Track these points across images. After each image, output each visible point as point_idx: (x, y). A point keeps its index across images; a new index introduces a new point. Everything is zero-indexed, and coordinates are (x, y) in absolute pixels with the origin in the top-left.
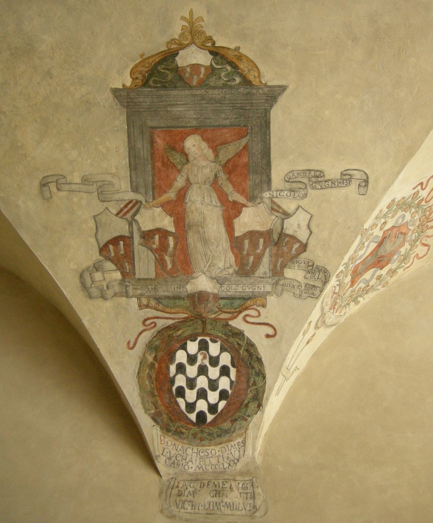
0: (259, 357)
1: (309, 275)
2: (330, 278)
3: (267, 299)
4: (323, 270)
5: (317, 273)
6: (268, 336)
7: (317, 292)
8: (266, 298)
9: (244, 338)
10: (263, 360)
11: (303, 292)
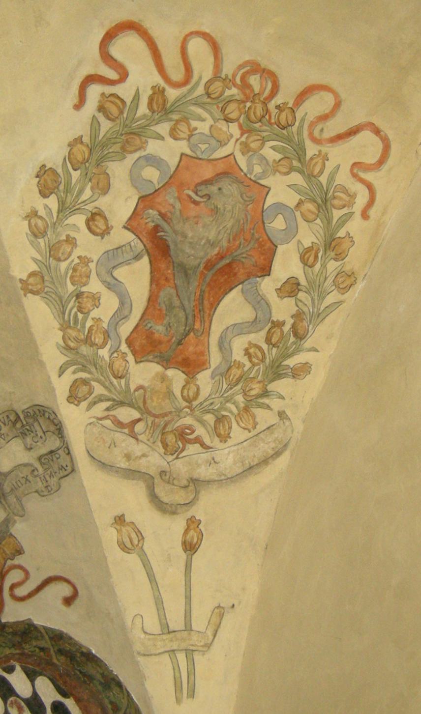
0: (84, 650)
1: (29, 440)
2: (59, 416)
3: (13, 533)
4: (37, 412)
5: (36, 424)
6: (68, 601)
7: (64, 460)
8: (11, 535)
9: (41, 632)
10: (94, 652)
11: (48, 478)
